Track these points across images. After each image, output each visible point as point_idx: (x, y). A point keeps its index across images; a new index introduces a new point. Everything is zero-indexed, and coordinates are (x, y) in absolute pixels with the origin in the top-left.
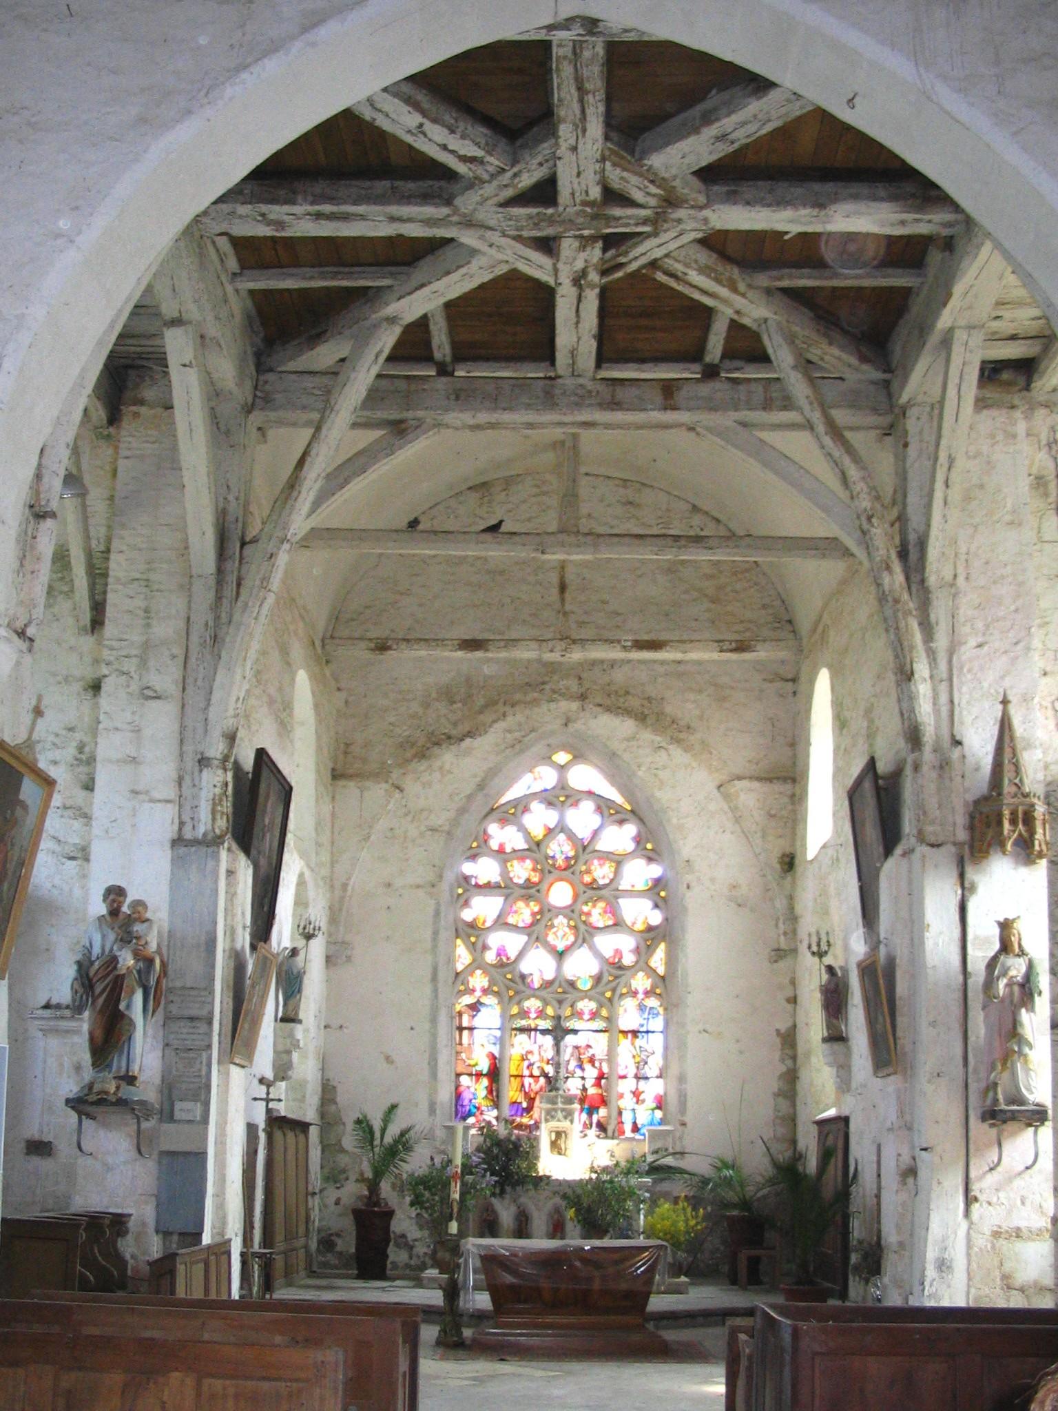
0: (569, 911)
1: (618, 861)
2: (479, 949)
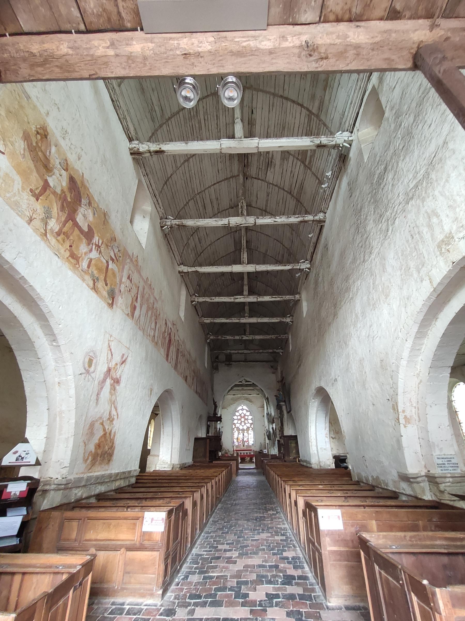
0: (244, 422)
1: (248, 416)
2: (235, 426)
